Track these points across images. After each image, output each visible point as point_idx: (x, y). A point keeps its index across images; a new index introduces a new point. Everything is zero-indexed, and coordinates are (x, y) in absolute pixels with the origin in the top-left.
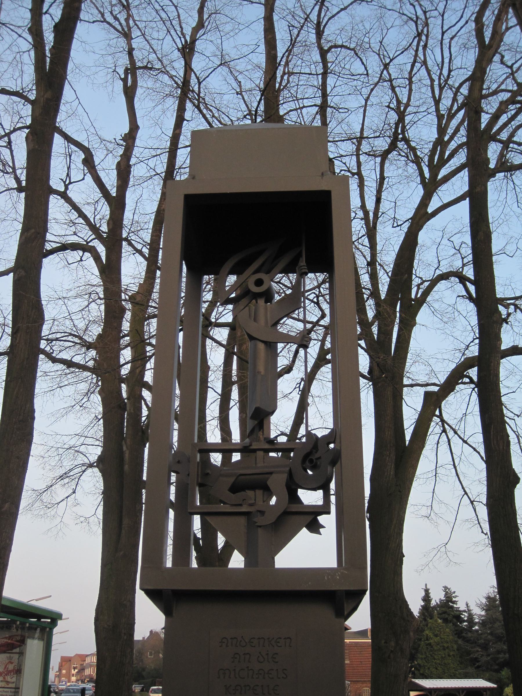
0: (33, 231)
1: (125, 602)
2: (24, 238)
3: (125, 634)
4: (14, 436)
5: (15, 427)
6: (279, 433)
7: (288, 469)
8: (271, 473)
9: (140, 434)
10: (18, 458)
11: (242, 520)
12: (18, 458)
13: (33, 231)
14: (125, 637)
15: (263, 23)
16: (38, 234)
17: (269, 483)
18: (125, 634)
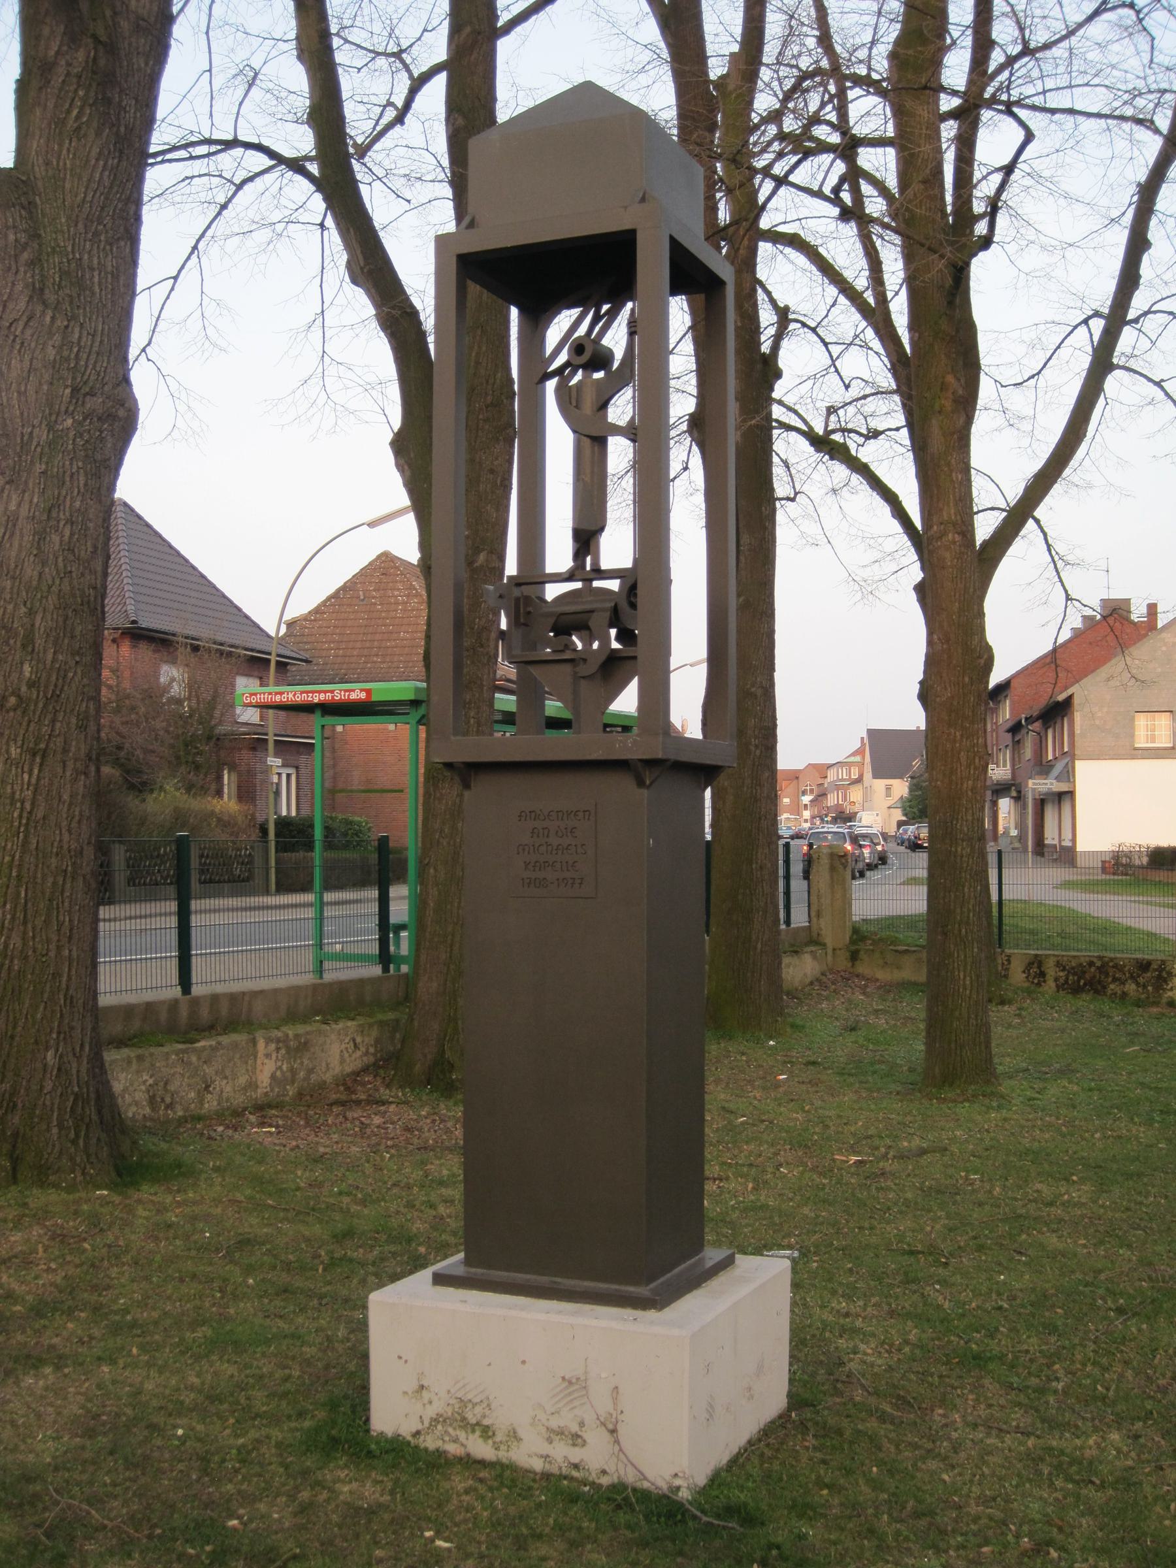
0: (468, 29)
1: (753, 690)
2: (453, 46)
3: (756, 746)
4: (480, 433)
5: (481, 417)
6: (1090, 313)
7: (613, 604)
8: (592, 611)
9: (759, 366)
10: (492, 471)
11: (567, 668)
12: (492, 471)
13: (468, 29)
14: (758, 752)
15: (376, 224)
16: (479, 33)
17: (590, 624)
18: (756, 746)
